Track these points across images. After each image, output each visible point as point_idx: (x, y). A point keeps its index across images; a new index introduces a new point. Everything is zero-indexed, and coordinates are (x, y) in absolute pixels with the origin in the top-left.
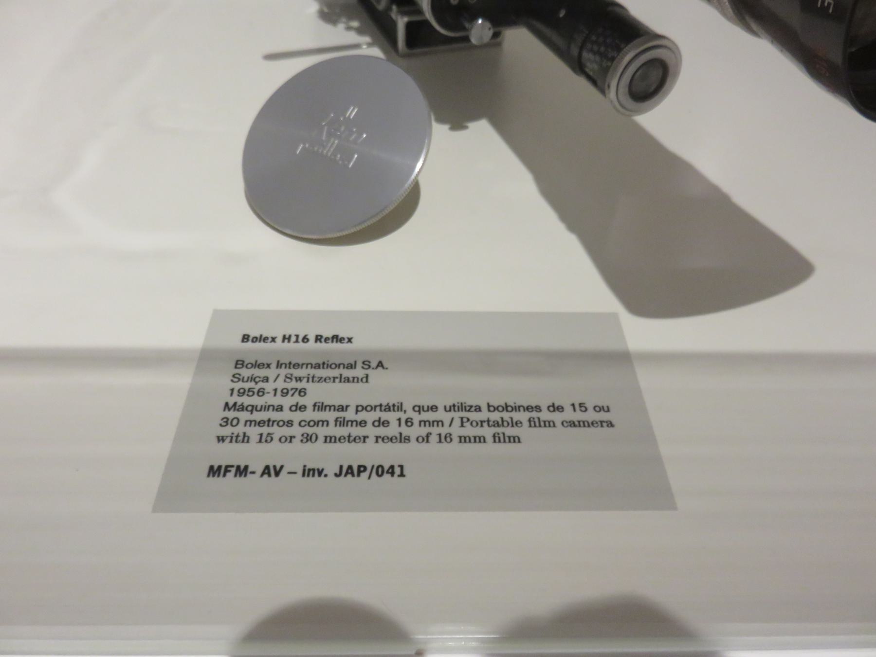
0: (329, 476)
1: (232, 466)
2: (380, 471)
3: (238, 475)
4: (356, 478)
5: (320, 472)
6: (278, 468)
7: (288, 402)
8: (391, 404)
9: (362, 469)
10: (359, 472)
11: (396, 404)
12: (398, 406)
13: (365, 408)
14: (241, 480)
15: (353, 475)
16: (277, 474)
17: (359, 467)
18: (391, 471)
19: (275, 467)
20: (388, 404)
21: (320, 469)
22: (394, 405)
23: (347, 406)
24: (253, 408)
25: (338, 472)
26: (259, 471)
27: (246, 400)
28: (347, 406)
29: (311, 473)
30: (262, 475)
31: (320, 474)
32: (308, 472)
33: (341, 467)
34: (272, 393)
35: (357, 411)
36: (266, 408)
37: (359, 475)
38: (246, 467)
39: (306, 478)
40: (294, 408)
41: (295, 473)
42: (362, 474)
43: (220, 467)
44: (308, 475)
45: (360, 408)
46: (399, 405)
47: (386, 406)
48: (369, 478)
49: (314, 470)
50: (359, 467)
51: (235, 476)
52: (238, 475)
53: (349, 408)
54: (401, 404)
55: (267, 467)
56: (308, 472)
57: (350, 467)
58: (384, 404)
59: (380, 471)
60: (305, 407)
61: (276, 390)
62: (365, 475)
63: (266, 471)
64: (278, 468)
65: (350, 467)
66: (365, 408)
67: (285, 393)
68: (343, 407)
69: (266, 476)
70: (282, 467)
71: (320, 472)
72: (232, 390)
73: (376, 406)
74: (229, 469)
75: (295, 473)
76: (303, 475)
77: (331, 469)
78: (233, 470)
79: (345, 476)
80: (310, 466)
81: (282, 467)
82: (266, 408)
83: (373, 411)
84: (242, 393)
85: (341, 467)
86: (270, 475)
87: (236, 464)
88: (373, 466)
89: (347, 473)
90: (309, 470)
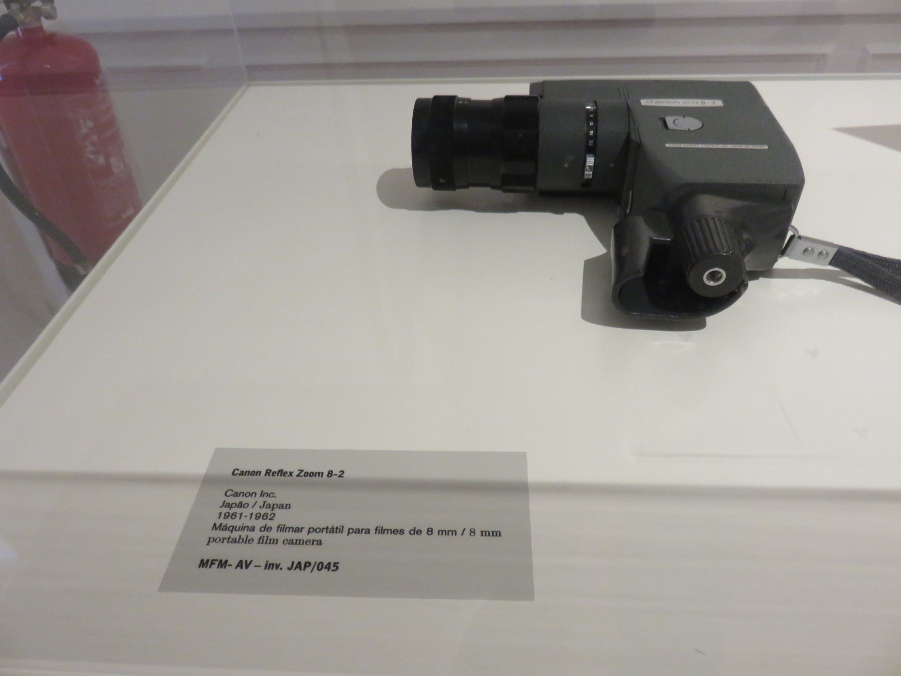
0: (283, 569)
1: (217, 560)
2: (320, 566)
3: (220, 568)
4: (302, 571)
5: (277, 567)
6: (248, 563)
7: (261, 523)
8: (335, 528)
9: (308, 564)
11: (339, 528)
12: (340, 529)
13: (315, 530)
15: (301, 569)
16: (247, 567)
18: (328, 567)
19: (246, 561)
20: (333, 527)
22: (337, 528)
23: (302, 528)
24: (234, 528)
25: (290, 566)
26: (235, 563)
27: (230, 522)
28: (302, 528)
29: (271, 566)
30: (236, 568)
31: (277, 568)
32: (270, 566)
34: (249, 516)
35: (309, 532)
36: (242, 528)
37: (304, 569)
38: (226, 561)
40: (263, 529)
41: (260, 566)
42: (307, 569)
43: (208, 561)
44: (269, 569)
45: (312, 530)
46: (341, 528)
47: (331, 529)
49: (273, 564)
50: (306, 563)
51: (218, 567)
52: (220, 568)
53: (303, 530)
54: (343, 527)
55: (241, 562)
56: (270, 566)
57: (299, 563)
58: (330, 527)
59: (320, 566)
60: (271, 528)
61: (252, 514)
62: (309, 569)
63: (240, 565)
64: (248, 563)
65: (299, 563)
66: (315, 530)
67: (258, 517)
68: (299, 528)
69: (239, 568)
70: (251, 562)
71: (277, 567)
72: (220, 514)
73: (323, 529)
74: (214, 562)
75: (260, 566)
76: (265, 568)
77: (286, 564)
78: (217, 563)
79: (295, 569)
80: (270, 562)
81: (251, 562)
82: (242, 528)
83: (321, 533)
84: (227, 516)
86: (242, 568)
87: (219, 559)
88: (316, 563)
89: (297, 567)
90: (270, 565)
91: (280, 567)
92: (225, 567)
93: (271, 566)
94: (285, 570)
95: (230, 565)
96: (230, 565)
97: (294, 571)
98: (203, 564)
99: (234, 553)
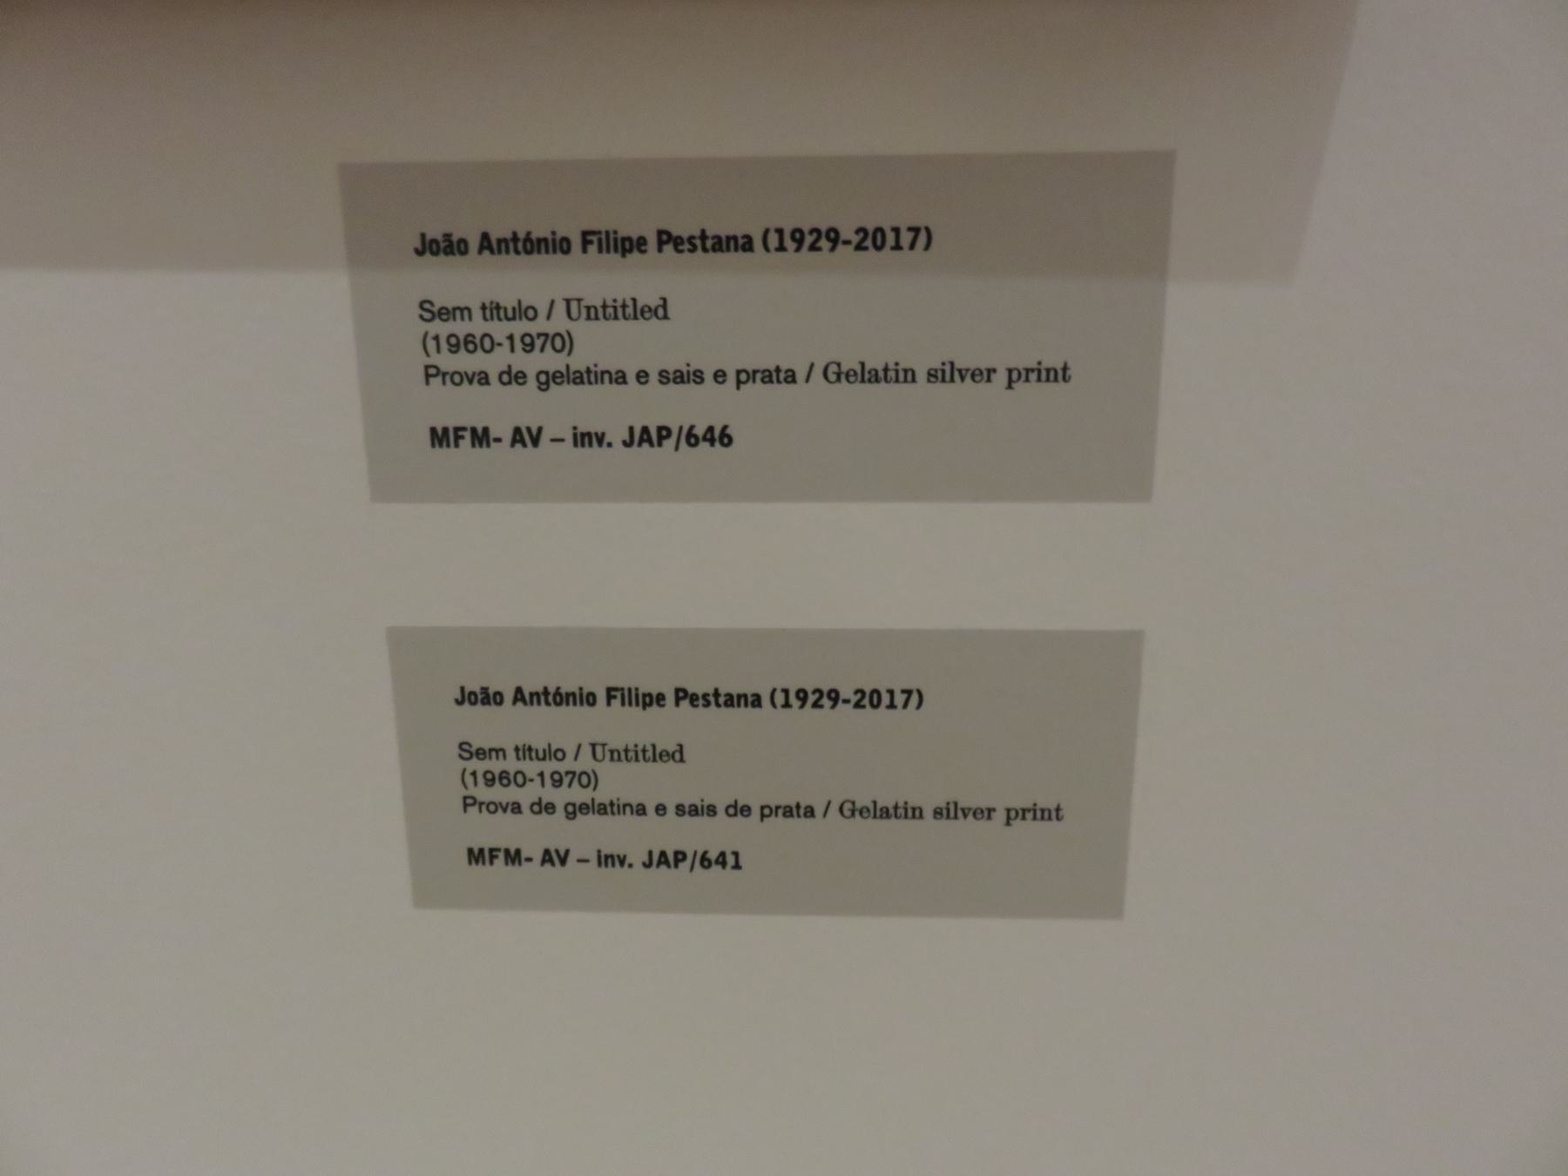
4: (656, 449)
5: (601, 440)
6: (534, 432)
10: (661, 439)
15: (651, 444)
17: (660, 429)
19: (529, 429)
25: (627, 437)
26: (507, 436)
30: (513, 445)
33: (631, 429)
37: (660, 444)
39: (580, 450)
41: (562, 440)
42: (665, 442)
43: (445, 430)
48: (677, 448)
50: (660, 429)
55: (517, 431)
56: (583, 439)
57: (645, 430)
62: (669, 444)
63: (518, 437)
64: (534, 432)
65: (645, 430)
75: (562, 440)
76: (575, 445)
77: (617, 434)
79: (640, 444)
80: (582, 429)
85: (631, 429)
86: (525, 445)
88: (681, 428)
90: (583, 435)
92: (488, 445)
94: (618, 445)
95: (498, 440)
96: (498, 440)
97: (639, 449)
98: (440, 437)
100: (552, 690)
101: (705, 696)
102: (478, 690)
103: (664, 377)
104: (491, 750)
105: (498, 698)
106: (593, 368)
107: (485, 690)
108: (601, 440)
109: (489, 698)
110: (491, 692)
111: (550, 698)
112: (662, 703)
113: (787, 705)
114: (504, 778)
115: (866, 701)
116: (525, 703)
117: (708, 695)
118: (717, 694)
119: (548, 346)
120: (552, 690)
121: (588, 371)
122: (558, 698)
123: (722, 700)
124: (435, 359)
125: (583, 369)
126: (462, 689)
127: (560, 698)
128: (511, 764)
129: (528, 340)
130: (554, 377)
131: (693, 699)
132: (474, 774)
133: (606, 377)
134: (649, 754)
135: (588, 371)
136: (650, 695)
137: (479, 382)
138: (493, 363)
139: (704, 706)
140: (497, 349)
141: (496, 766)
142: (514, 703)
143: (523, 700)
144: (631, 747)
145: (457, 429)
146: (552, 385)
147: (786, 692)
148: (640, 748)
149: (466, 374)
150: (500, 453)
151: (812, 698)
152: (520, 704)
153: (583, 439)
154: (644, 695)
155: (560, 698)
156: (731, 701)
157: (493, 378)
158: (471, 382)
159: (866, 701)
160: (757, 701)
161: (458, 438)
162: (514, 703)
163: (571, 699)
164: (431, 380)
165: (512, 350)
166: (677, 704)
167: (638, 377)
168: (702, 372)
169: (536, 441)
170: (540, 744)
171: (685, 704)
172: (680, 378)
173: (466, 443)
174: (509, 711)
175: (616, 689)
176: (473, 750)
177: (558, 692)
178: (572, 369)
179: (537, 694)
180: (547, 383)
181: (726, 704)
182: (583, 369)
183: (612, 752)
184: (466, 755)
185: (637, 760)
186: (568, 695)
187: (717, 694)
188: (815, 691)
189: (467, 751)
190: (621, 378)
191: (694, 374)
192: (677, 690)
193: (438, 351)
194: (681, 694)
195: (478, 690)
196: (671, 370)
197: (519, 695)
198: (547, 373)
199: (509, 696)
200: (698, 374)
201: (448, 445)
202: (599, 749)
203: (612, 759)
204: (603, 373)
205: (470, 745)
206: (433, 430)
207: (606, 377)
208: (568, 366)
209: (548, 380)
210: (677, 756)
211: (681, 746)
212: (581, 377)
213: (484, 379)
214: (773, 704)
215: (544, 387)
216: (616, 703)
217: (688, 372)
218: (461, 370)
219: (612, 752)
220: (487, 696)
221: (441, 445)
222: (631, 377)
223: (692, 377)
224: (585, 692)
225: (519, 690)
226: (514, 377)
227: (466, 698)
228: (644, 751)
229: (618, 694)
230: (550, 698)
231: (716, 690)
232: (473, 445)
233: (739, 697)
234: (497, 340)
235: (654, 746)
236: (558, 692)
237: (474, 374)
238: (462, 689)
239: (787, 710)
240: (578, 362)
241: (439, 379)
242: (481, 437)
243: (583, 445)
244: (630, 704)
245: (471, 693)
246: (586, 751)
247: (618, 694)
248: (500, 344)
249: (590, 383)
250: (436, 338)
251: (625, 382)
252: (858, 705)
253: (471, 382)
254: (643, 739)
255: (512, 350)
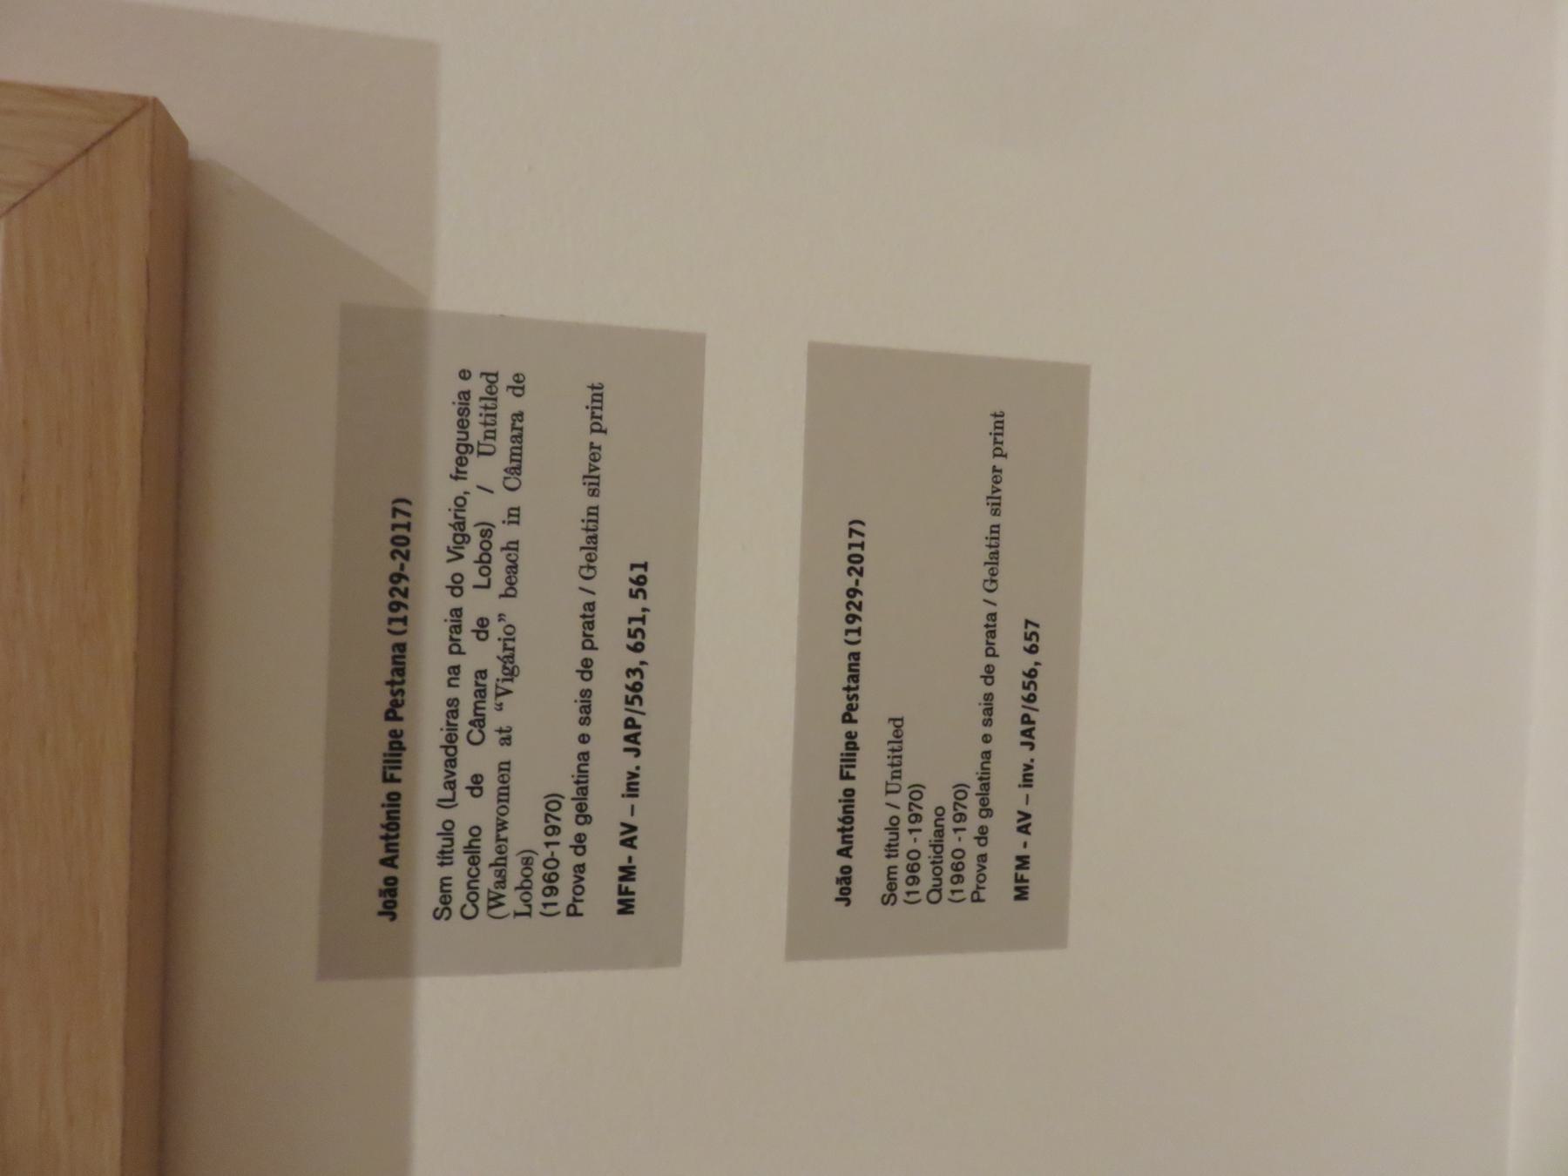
4: (643, 730)
5: (633, 775)
14: (639, 873)
17: (627, 727)
19: (623, 833)
21: (629, 776)
26: (628, 851)
33: (626, 750)
37: (639, 727)
41: (633, 807)
43: (620, 902)
48: (643, 714)
49: (629, 784)
50: (627, 727)
52: (632, 877)
55: (623, 843)
56: (632, 790)
57: (627, 738)
62: (639, 719)
63: (628, 843)
65: (627, 738)
71: (633, 775)
75: (633, 807)
76: (637, 796)
77: (630, 762)
79: (639, 743)
80: (623, 789)
85: (626, 750)
86: (635, 838)
88: (627, 709)
90: (629, 789)
91: (634, 770)
92: (634, 867)
93: (633, 787)
94: (638, 762)
95: (630, 859)
96: (630, 859)
99: (605, 856)
100: (840, 825)
101: (849, 698)
102: (839, 887)
103: (585, 721)
104: (889, 879)
105: (846, 870)
106: (575, 779)
107: (838, 881)
108: (634, 775)
109: (845, 876)
110: (840, 876)
111: (848, 826)
112: (853, 734)
113: (858, 631)
114: (913, 868)
115: (858, 567)
116: (851, 848)
117: (848, 696)
118: (848, 689)
119: (556, 814)
120: (840, 825)
121: (577, 782)
122: (848, 820)
123: (853, 685)
124: (562, 907)
125: (576, 786)
126: (837, 899)
127: (847, 818)
128: (901, 862)
129: (550, 831)
130: (581, 811)
131: (851, 708)
132: (908, 893)
133: (583, 768)
134: (896, 746)
135: (577, 782)
136: (847, 744)
137: (582, 872)
138: (568, 859)
139: (857, 699)
140: (556, 856)
141: (902, 874)
142: (850, 857)
143: (848, 849)
144: (890, 761)
145: (620, 893)
146: (587, 813)
147: (847, 632)
148: (890, 753)
149: (575, 882)
150: (641, 858)
151: (854, 611)
152: (851, 852)
153: (632, 790)
154: (847, 749)
155: (847, 818)
156: (854, 676)
157: (580, 860)
158: (582, 879)
159: (858, 567)
160: (855, 656)
161: (627, 892)
162: (850, 857)
163: (848, 809)
164: (579, 911)
165: (558, 843)
166: (855, 721)
167: (584, 742)
168: (583, 691)
169: (633, 828)
170: (886, 837)
171: (855, 715)
172: (586, 708)
173: (631, 886)
174: (857, 861)
175: (841, 771)
176: (888, 893)
177: (843, 820)
178: (575, 795)
179: (843, 837)
180: (585, 816)
181: (857, 681)
182: (576, 786)
183: (893, 777)
184: (892, 899)
185: (900, 757)
186: (845, 812)
187: (848, 689)
188: (848, 608)
189: (889, 899)
190: (584, 756)
191: (583, 696)
192: (844, 721)
193: (555, 904)
194: (848, 718)
195: (839, 887)
196: (580, 715)
197: (845, 852)
198: (578, 816)
199: (844, 861)
200: (583, 693)
201: (633, 900)
202: (891, 788)
203: (899, 777)
204: (579, 771)
205: (884, 895)
206: (621, 912)
207: (583, 768)
208: (573, 799)
209: (583, 816)
210: (898, 723)
211: (890, 720)
212: (581, 788)
213: (580, 868)
214: (858, 642)
215: (588, 819)
216: (852, 772)
217: (582, 701)
218: (572, 886)
219: (893, 777)
220: (843, 879)
221: (632, 906)
222: (584, 748)
223: (586, 699)
224: (842, 797)
225: (840, 852)
226: (580, 843)
227: (845, 897)
228: (893, 750)
229: (845, 770)
230: (848, 826)
231: (845, 689)
232: (633, 880)
233: (850, 670)
234: (549, 856)
235: (890, 742)
236: (843, 820)
237: (576, 876)
238: (837, 899)
239: (863, 631)
240: (569, 790)
241: (578, 904)
242: (627, 873)
243: (637, 790)
244: (854, 760)
245: (841, 893)
246: (892, 798)
247: (845, 770)
248: (553, 853)
249: (586, 782)
250: (545, 905)
251: (587, 753)
252: (861, 573)
253: (582, 879)
254: (884, 751)
255: (558, 843)
